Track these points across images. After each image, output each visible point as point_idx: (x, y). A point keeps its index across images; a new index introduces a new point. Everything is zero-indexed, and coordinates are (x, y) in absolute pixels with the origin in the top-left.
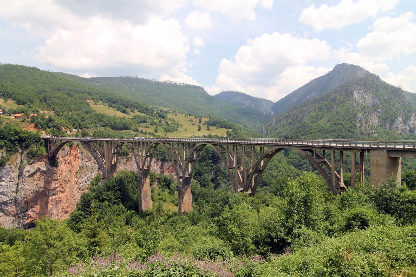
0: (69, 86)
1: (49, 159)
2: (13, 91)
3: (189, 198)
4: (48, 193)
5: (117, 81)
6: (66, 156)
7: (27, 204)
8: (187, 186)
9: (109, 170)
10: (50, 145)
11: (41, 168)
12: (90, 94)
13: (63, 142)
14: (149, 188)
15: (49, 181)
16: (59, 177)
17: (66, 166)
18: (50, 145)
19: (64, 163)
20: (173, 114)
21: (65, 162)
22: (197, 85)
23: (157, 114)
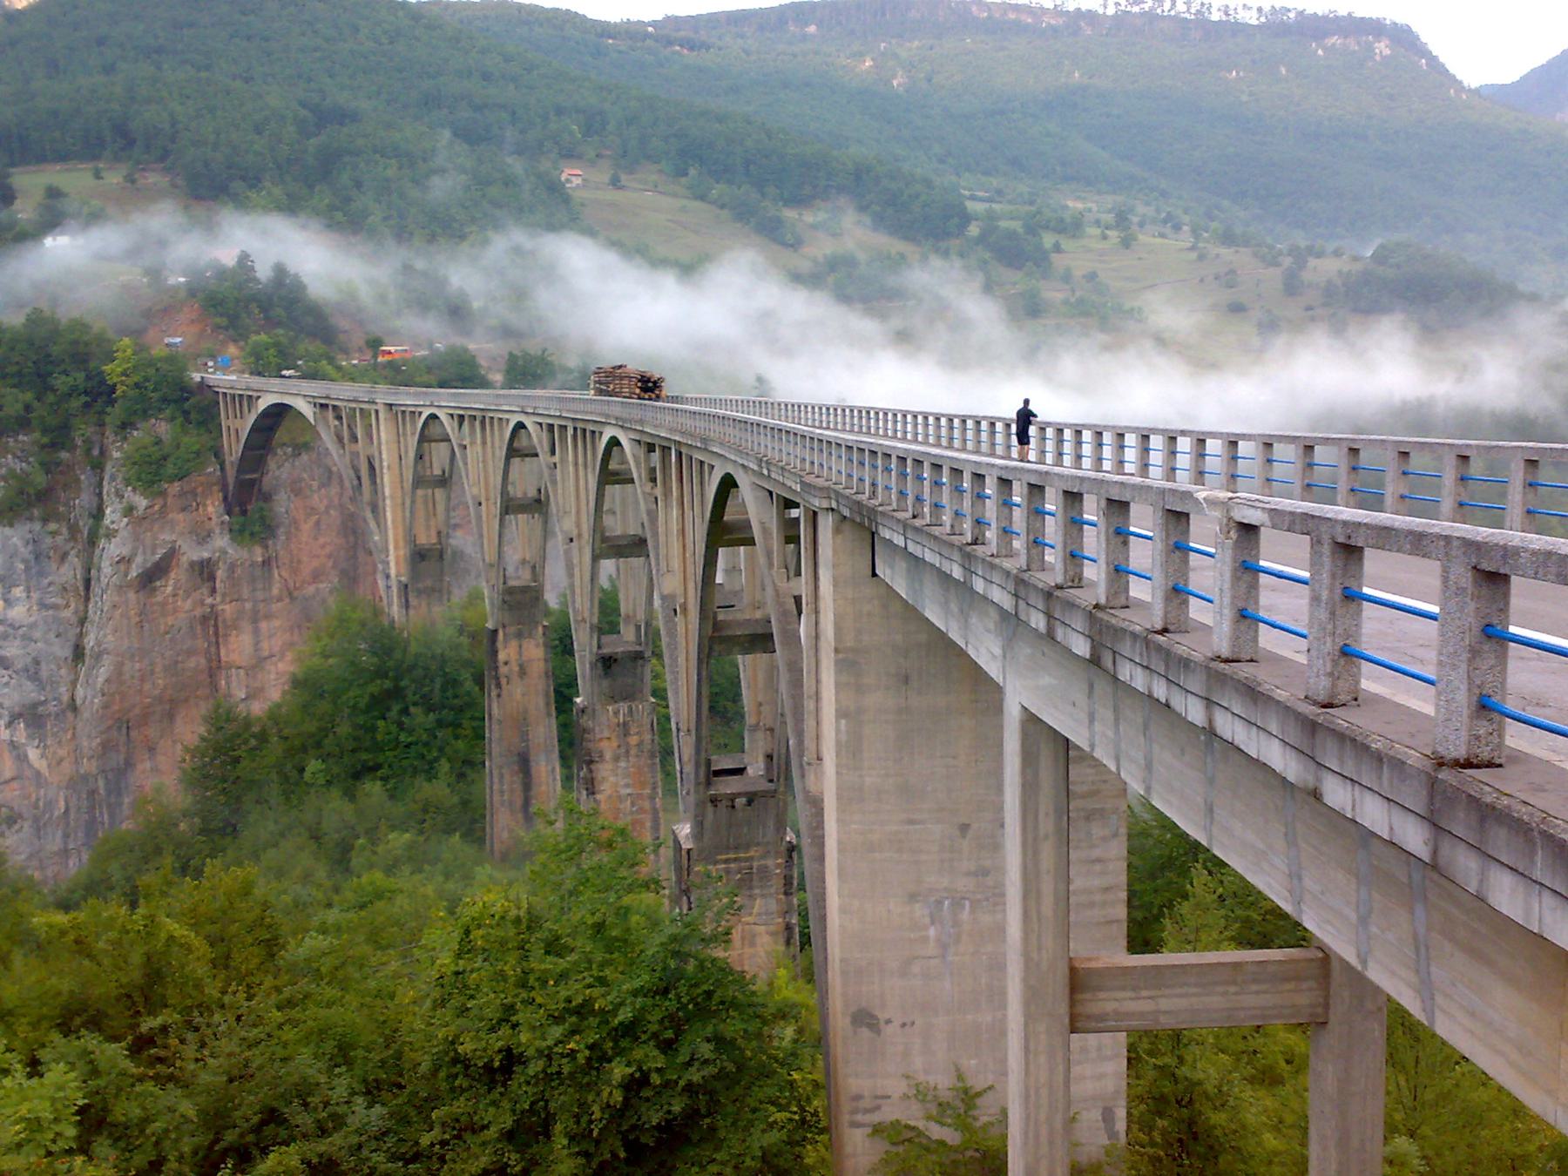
0: (486, 77)
1: (225, 499)
2: (173, 125)
3: (643, 785)
4: (228, 683)
5: (812, 29)
6: (319, 488)
7: (124, 731)
8: (623, 707)
9: (403, 579)
10: (230, 422)
11: (184, 548)
12: (593, 124)
13: (262, 405)
14: (548, 704)
15: (224, 621)
16: (280, 599)
17: (323, 547)
18: (230, 422)
19: (307, 527)
20: (1105, 237)
21: (318, 523)
22: (1358, 14)
23: (982, 239)
